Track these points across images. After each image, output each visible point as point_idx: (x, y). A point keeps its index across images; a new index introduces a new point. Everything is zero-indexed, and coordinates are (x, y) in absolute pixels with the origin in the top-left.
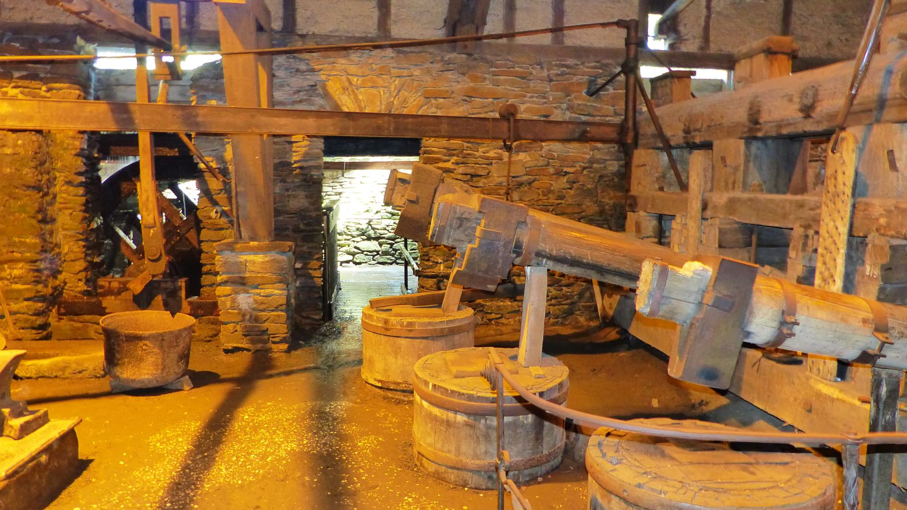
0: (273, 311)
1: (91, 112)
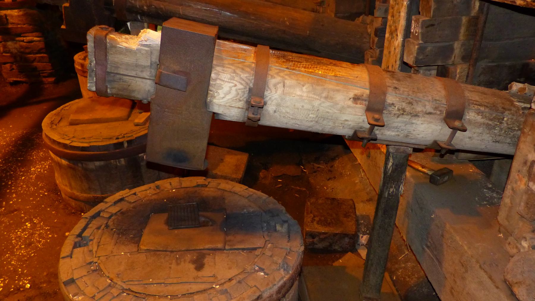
0: (37, 53)
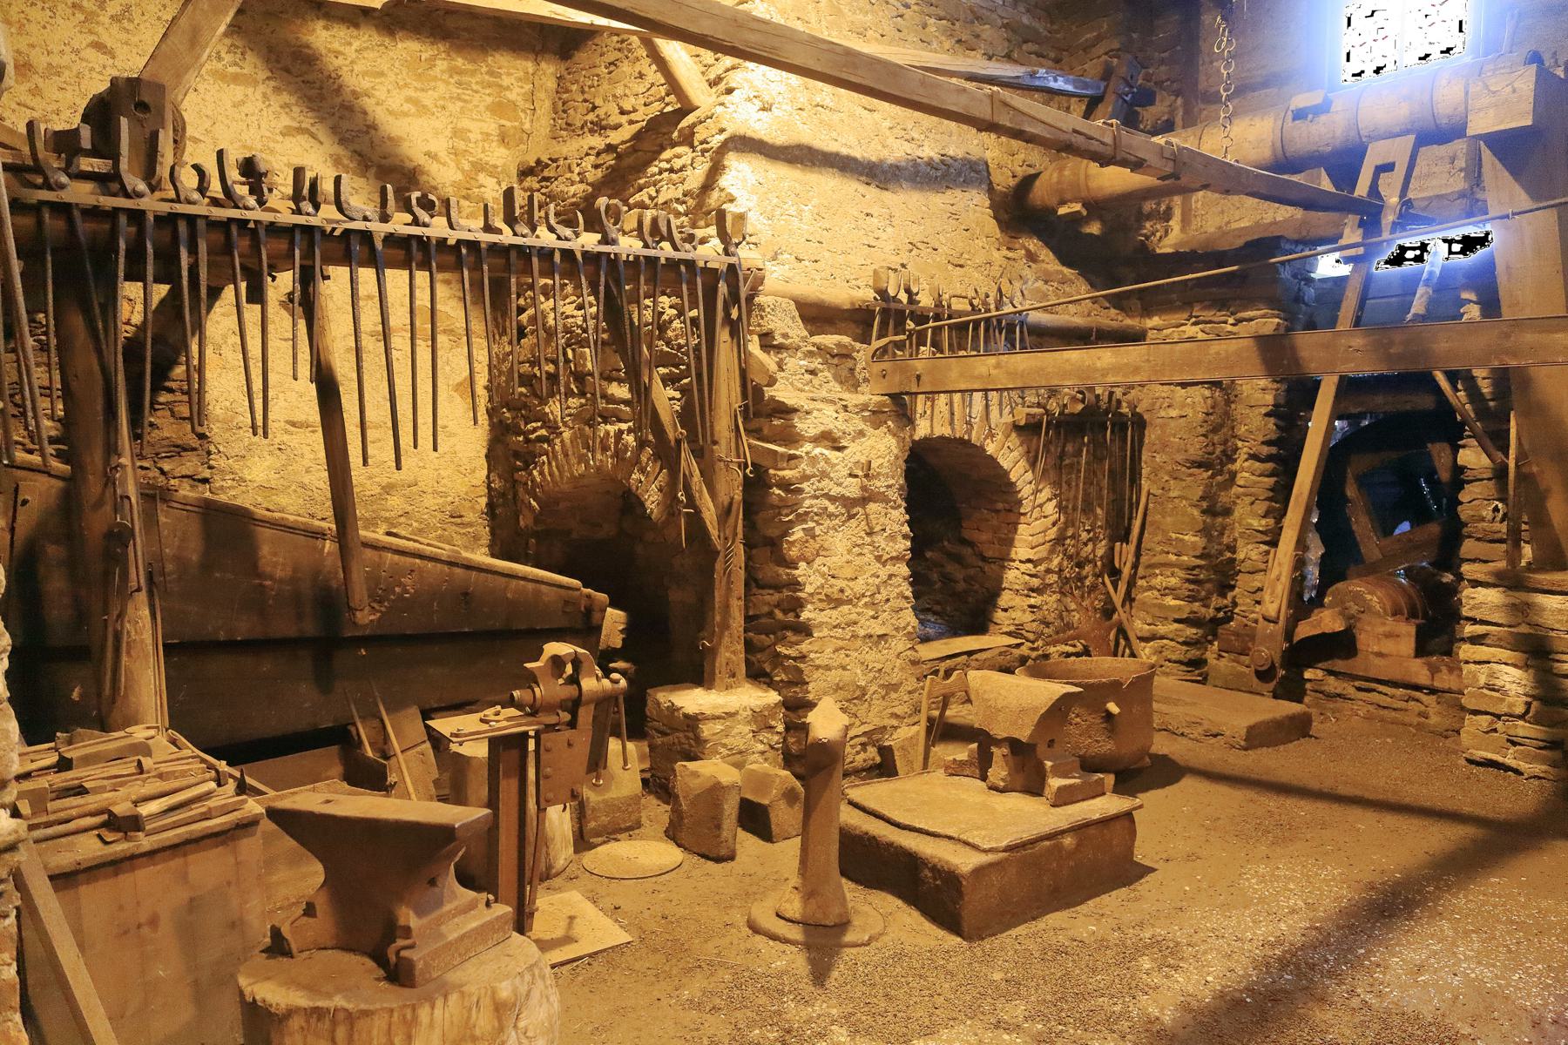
1: (1218, 353)
